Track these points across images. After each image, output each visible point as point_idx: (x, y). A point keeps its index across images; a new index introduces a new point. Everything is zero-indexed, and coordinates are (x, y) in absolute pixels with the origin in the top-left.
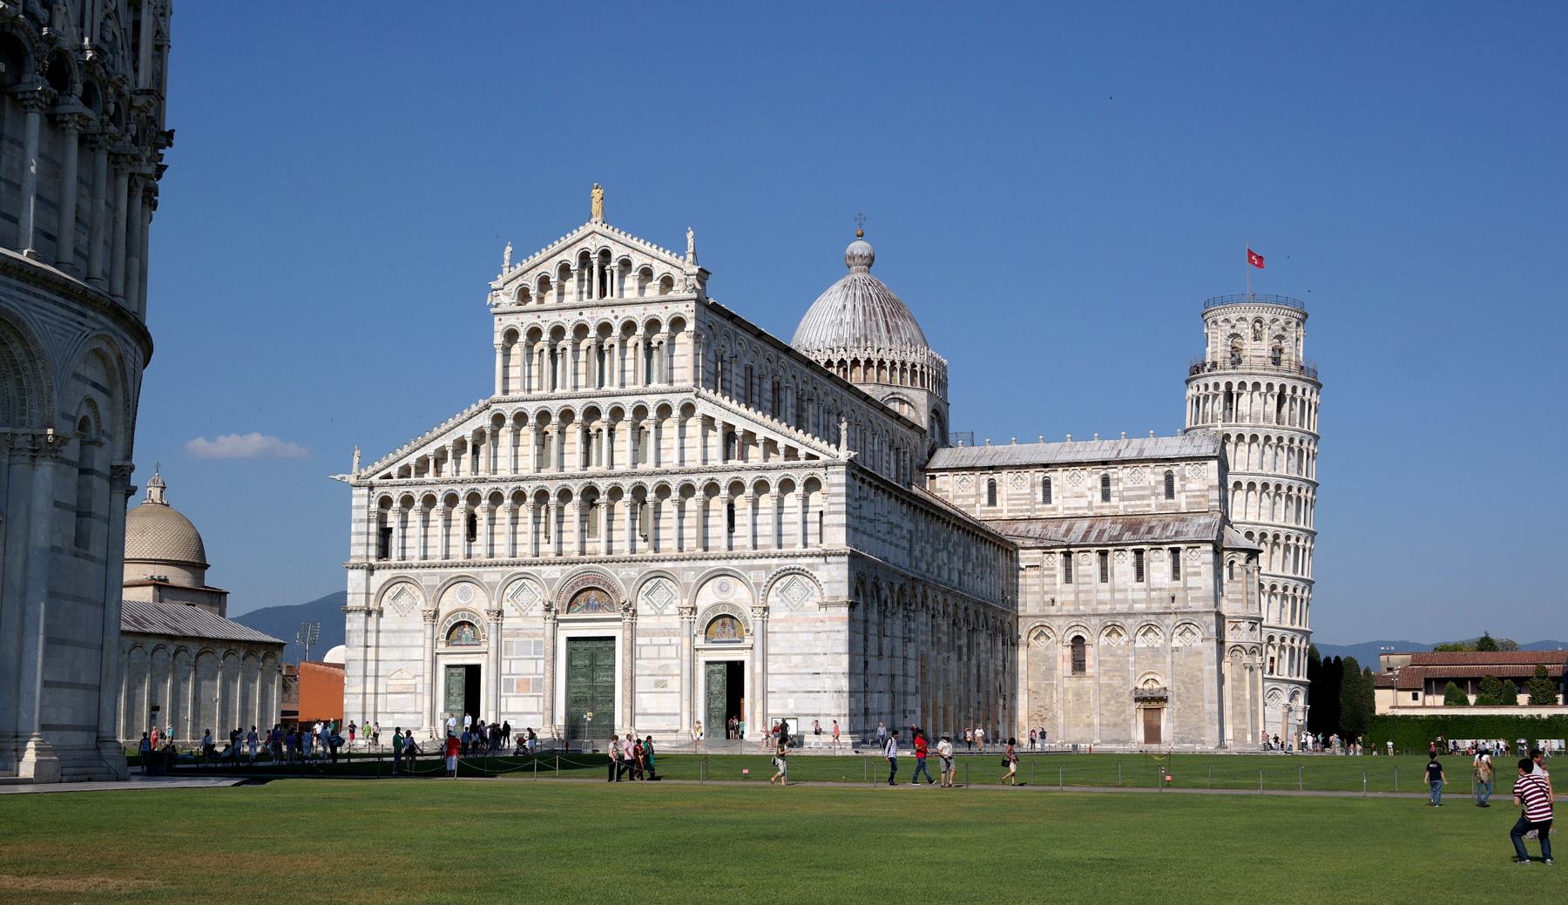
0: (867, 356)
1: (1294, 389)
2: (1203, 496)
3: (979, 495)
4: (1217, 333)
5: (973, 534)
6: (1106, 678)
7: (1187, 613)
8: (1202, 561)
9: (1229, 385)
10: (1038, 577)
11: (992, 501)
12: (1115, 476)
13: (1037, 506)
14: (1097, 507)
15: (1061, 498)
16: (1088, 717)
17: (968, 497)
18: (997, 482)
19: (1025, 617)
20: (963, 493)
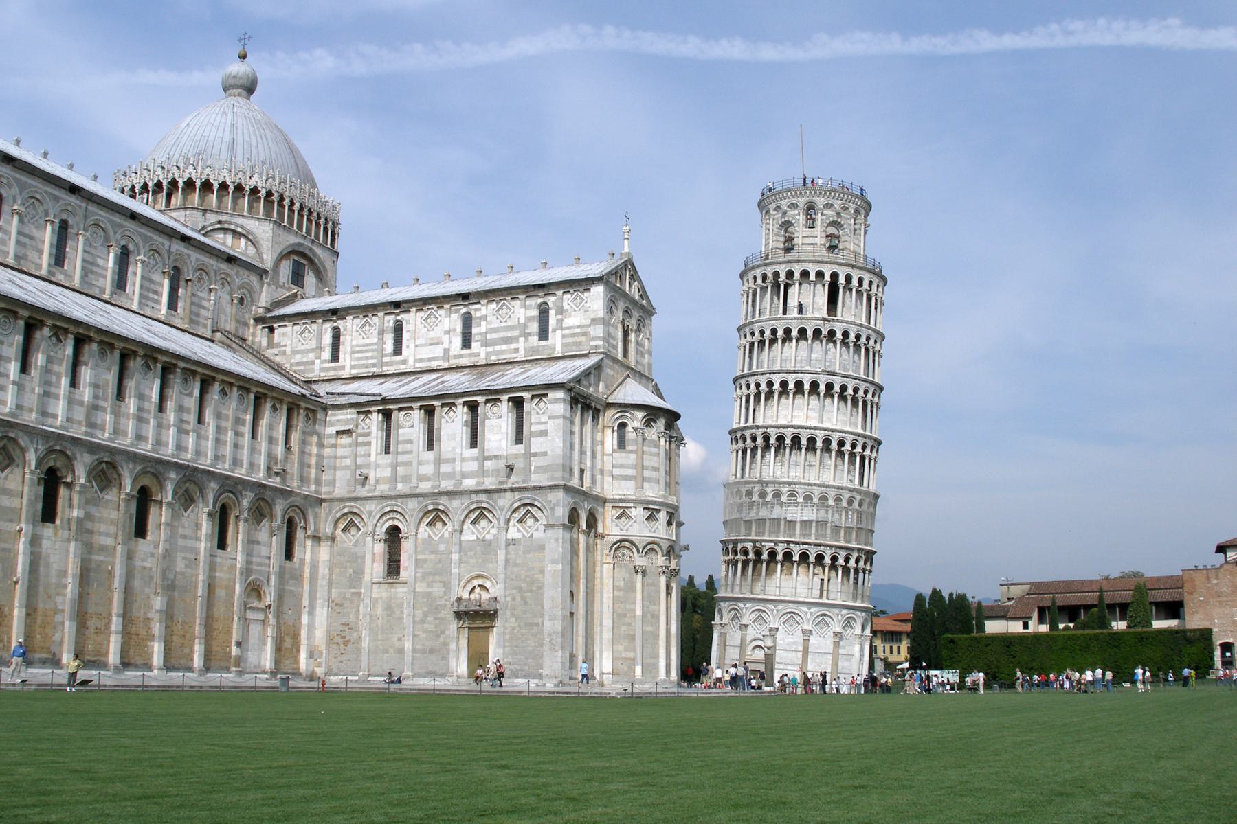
0: (188, 176)
1: (848, 279)
2: (584, 334)
3: (320, 348)
4: (769, 224)
5: (156, 360)
6: (424, 585)
7: (525, 489)
8: (549, 413)
9: (776, 274)
10: (351, 445)
11: (335, 357)
12: (478, 314)
13: (386, 359)
14: (455, 357)
15: (412, 346)
16: (400, 639)
17: (309, 351)
18: (342, 330)
19: (332, 500)
20: (303, 348)
